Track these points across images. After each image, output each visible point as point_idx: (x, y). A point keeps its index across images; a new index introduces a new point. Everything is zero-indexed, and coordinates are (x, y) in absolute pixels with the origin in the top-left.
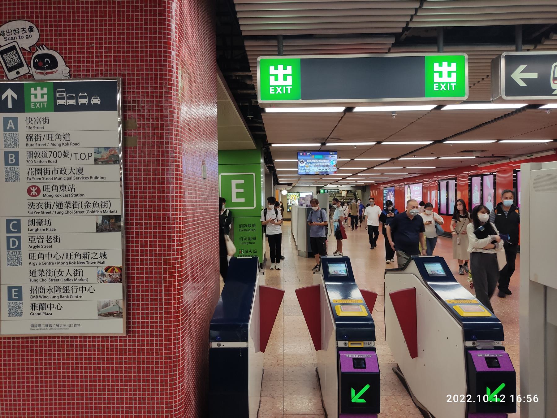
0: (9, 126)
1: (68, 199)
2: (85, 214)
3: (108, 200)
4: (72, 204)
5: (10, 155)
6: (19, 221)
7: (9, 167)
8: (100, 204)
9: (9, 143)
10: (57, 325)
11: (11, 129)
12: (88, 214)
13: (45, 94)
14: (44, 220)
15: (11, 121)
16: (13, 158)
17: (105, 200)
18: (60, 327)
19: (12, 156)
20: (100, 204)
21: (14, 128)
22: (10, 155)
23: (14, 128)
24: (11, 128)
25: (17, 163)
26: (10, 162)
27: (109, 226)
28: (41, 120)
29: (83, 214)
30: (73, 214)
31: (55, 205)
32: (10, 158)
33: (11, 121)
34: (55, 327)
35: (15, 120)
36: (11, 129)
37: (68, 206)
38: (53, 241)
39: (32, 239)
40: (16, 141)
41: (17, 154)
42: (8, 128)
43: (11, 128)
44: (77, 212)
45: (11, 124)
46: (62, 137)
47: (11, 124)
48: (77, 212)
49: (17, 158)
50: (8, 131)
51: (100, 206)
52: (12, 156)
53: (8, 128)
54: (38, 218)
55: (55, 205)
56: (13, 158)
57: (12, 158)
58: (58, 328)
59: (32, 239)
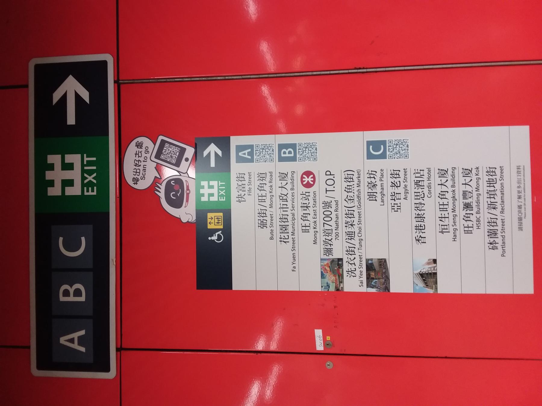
0: (246, 156)
1: (342, 224)
2: (362, 211)
3: (343, 173)
4: (349, 220)
5: (283, 155)
6: (369, 143)
7: (298, 156)
8: (349, 184)
9: (268, 157)
10: (519, 197)
11: (251, 154)
12: (362, 207)
13: (209, 183)
14: (369, 180)
15: (240, 154)
16: (287, 152)
17: (344, 177)
18: (522, 194)
19: (285, 153)
20: (349, 184)
21: (250, 150)
22: (283, 155)
23: (250, 150)
24: (249, 154)
25: (293, 146)
26: (292, 155)
27: (379, 279)
28: (240, 183)
29: (362, 213)
30: (363, 226)
31: (349, 241)
32: (287, 155)
33: (240, 154)
34: (522, 200)
35: (240, 148)
36: (251, 154)
37: (352, 225)
38: (398, 179)
39: (396, 208)
40: (265, 147)
41: (281, 147)
42: (250, 157)
43: (249, 154)
44: (360, 222)
45: (245, 154)
46: (262, 182)
47: (245, 154)
48: (360, 222)
49: (287, 146)
50: (253, 157)
51: (351, 184)
52: (285, 153)
53: (250, 157)
54: (366, 188)
55: (349, 241)
56: (287, 152)
57: (287, 153)
58: (523, 197)
59: (396, 208)
